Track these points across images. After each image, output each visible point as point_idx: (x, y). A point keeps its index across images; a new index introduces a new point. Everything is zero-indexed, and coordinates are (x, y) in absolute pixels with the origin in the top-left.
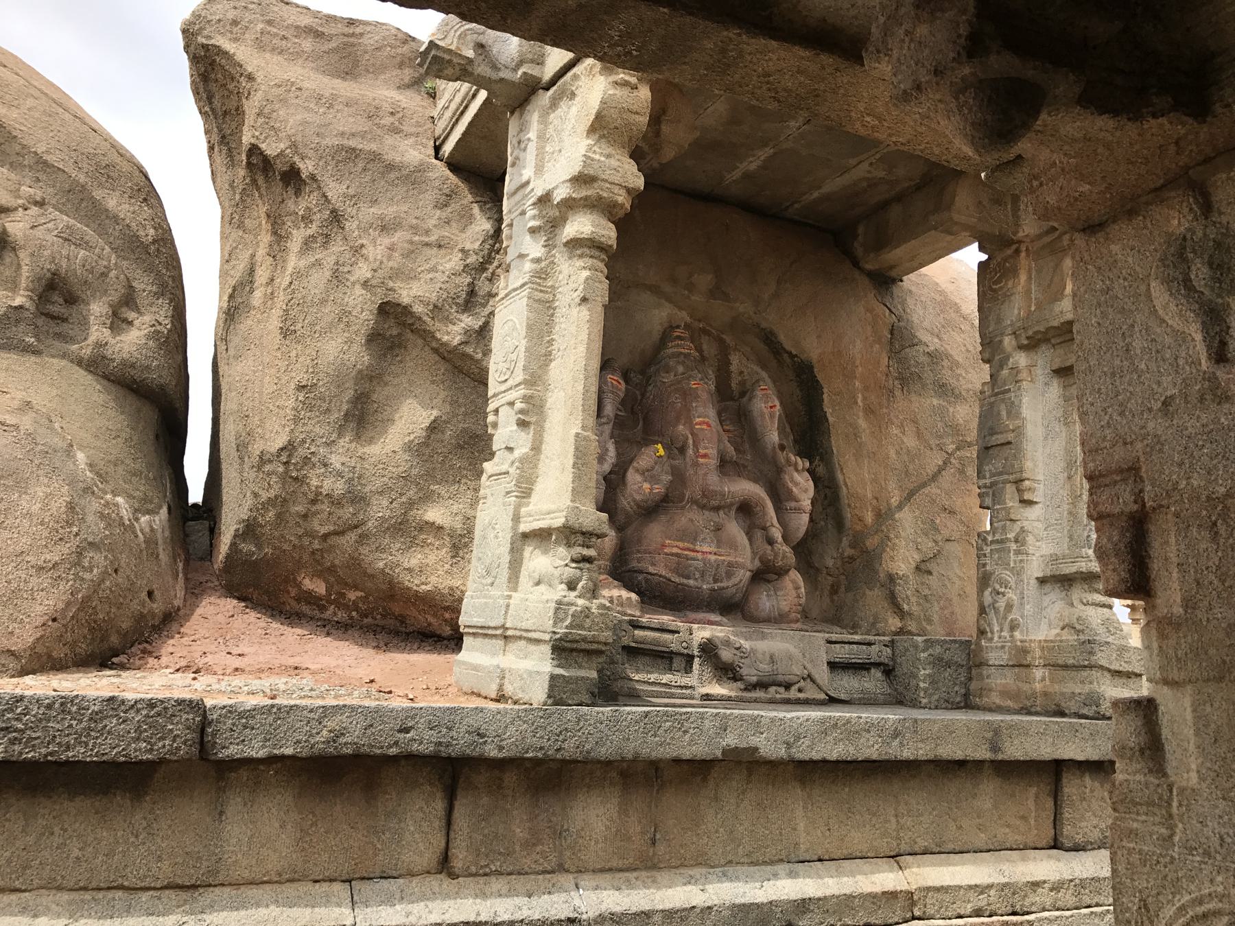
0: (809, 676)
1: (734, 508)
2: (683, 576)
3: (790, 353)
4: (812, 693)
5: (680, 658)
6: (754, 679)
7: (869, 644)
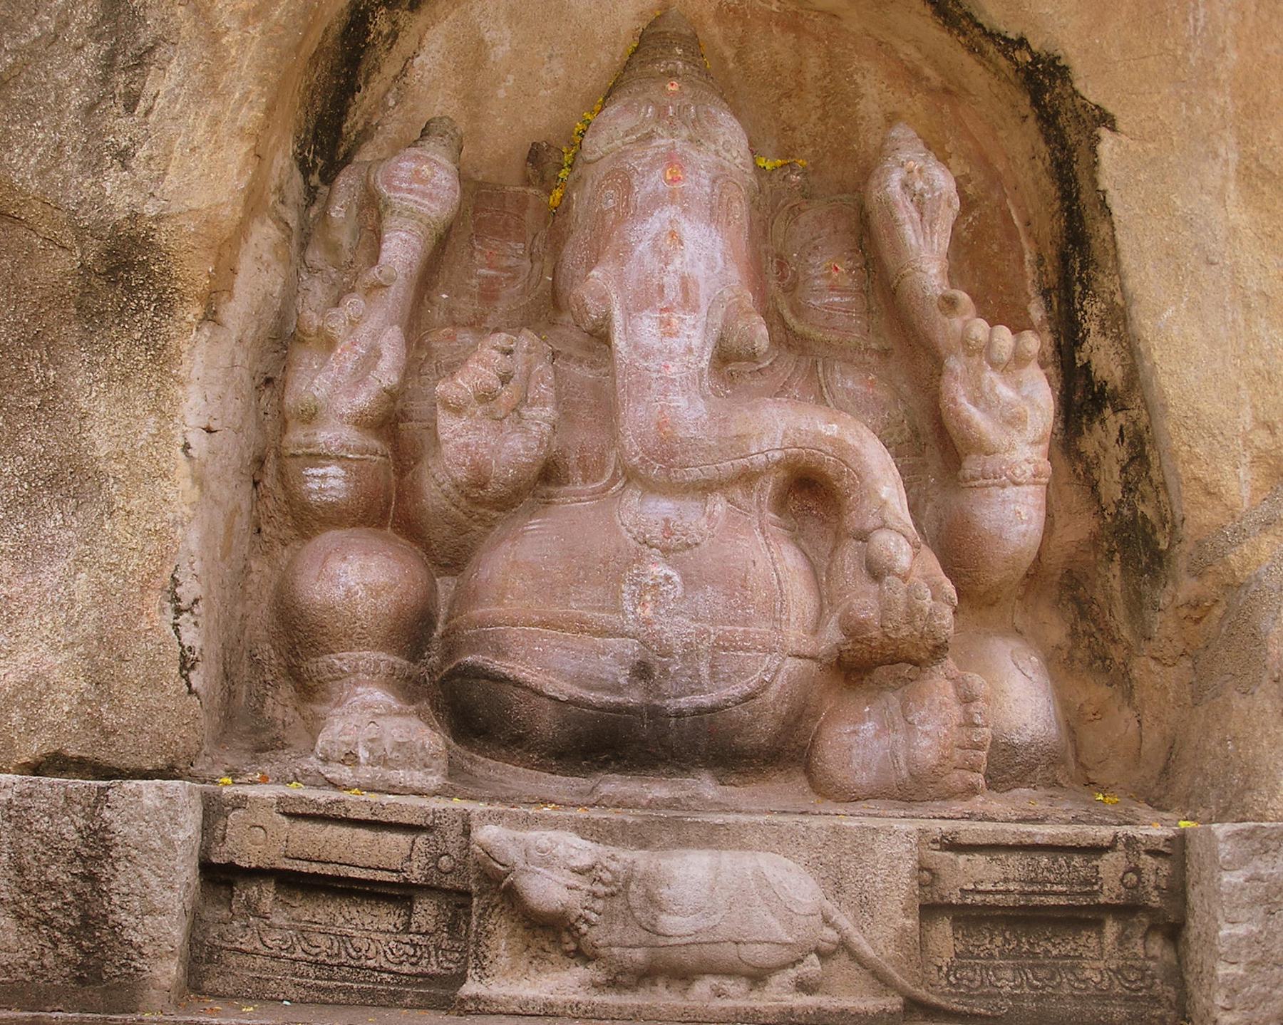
1: (768, 486)
6: (639, 955)
7: (1097, 850)
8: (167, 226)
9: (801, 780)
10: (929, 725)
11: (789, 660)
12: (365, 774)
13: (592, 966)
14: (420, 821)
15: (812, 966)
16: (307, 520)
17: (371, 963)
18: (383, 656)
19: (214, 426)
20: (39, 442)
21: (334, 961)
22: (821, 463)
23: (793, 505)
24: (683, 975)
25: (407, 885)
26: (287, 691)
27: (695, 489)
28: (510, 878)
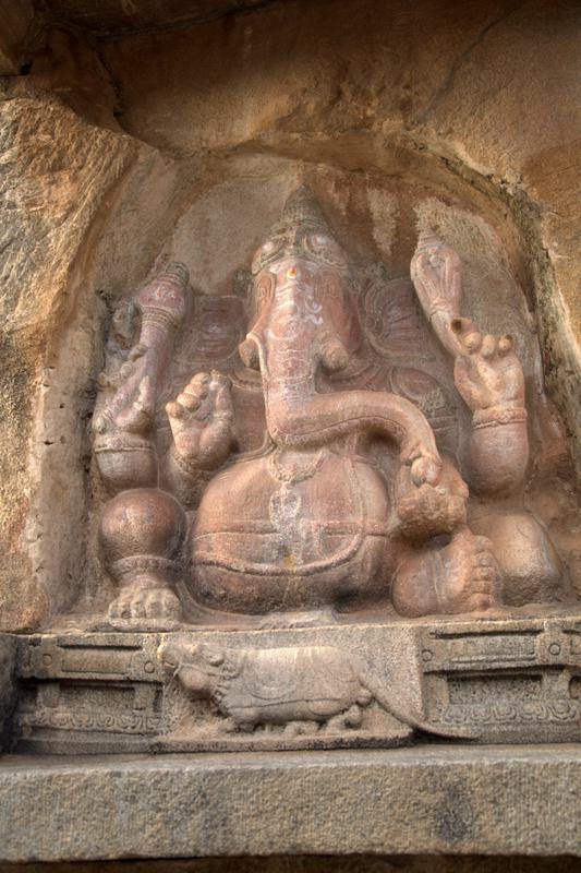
0: (373, 699)
2: (251, 559)
4: (381, 728)
5: (147, 688)
6: (252, 712)
8: (15, 336)
9: (390, 608)
10: (459, 567)
12: (134, 621)
13: (226, 720)
15: (354, 713)
16: (114, 487)
17: (110, 728)
18: (150, 557)
19: (50, 441)
21: (90, 729)
22: (382, 424)
23: (375, 450)
24: (279, 722)
26: (107, 582)
27: (312, 447)
28: (175, 673)
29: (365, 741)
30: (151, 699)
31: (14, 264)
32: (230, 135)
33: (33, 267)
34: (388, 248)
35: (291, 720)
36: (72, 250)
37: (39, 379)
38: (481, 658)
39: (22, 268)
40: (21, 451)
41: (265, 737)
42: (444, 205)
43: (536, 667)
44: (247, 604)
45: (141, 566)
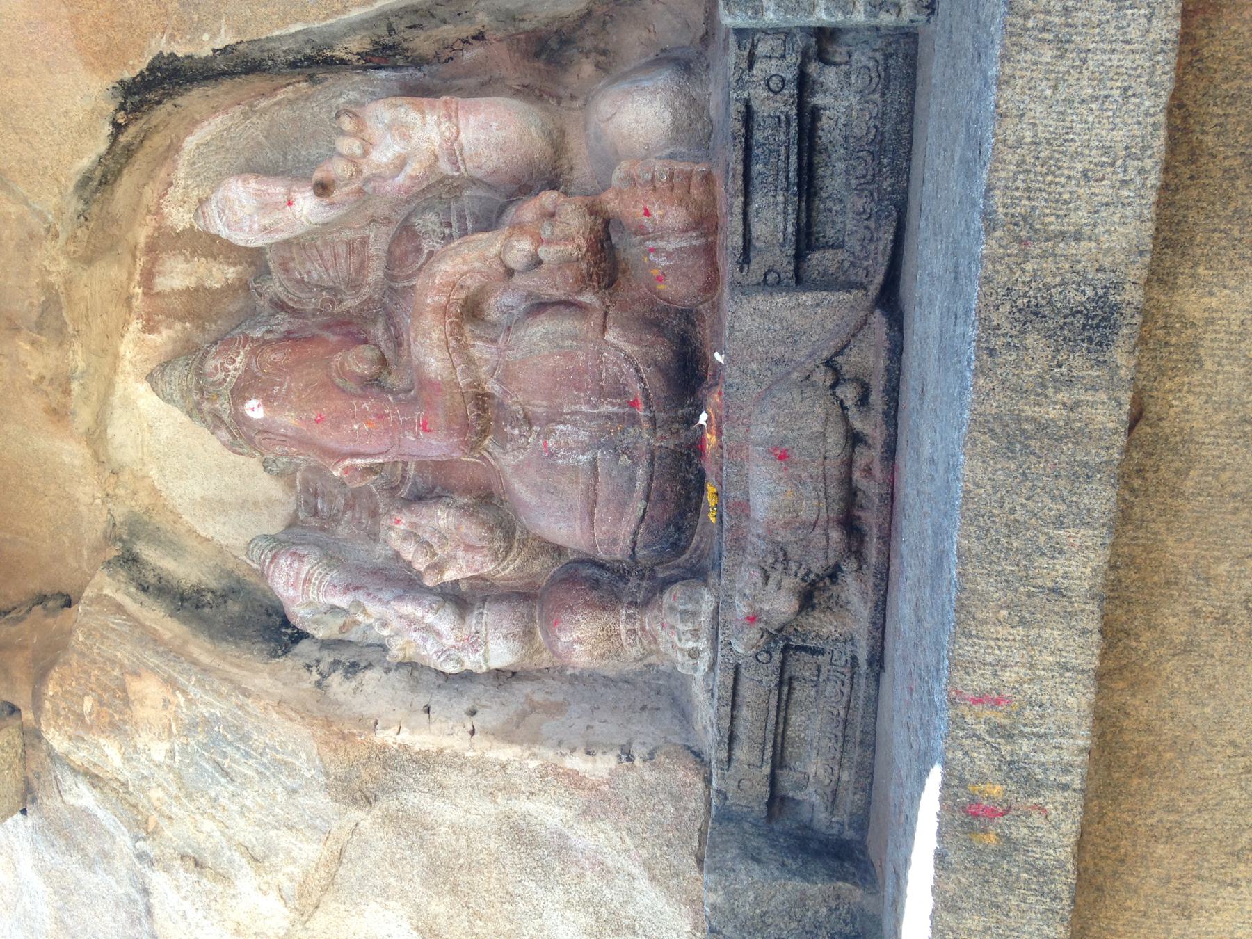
0: (829, 364)
3: (114, 137)
11: (607, 337)
14: (731, 672)
15: (848, 393)
19: (470, 728)
20: (489, 837)
21: (841, 739)
24: (851, 495)
25: (780, 684)
29: (889, 380)
30: (807, 657)
31: (243, 760)
32: (83, 468)
33: (245, 738)
34: (232, 270)
35: (851, 479)
36: (224, 689)
37: (390, 741)
38: (780, 198)
39: (247, 753)
40: (481, 766)
41: (870, 519)
42: (171, 190)
43: (800, 115)
44: (688, 498)
45: (634, 624)
